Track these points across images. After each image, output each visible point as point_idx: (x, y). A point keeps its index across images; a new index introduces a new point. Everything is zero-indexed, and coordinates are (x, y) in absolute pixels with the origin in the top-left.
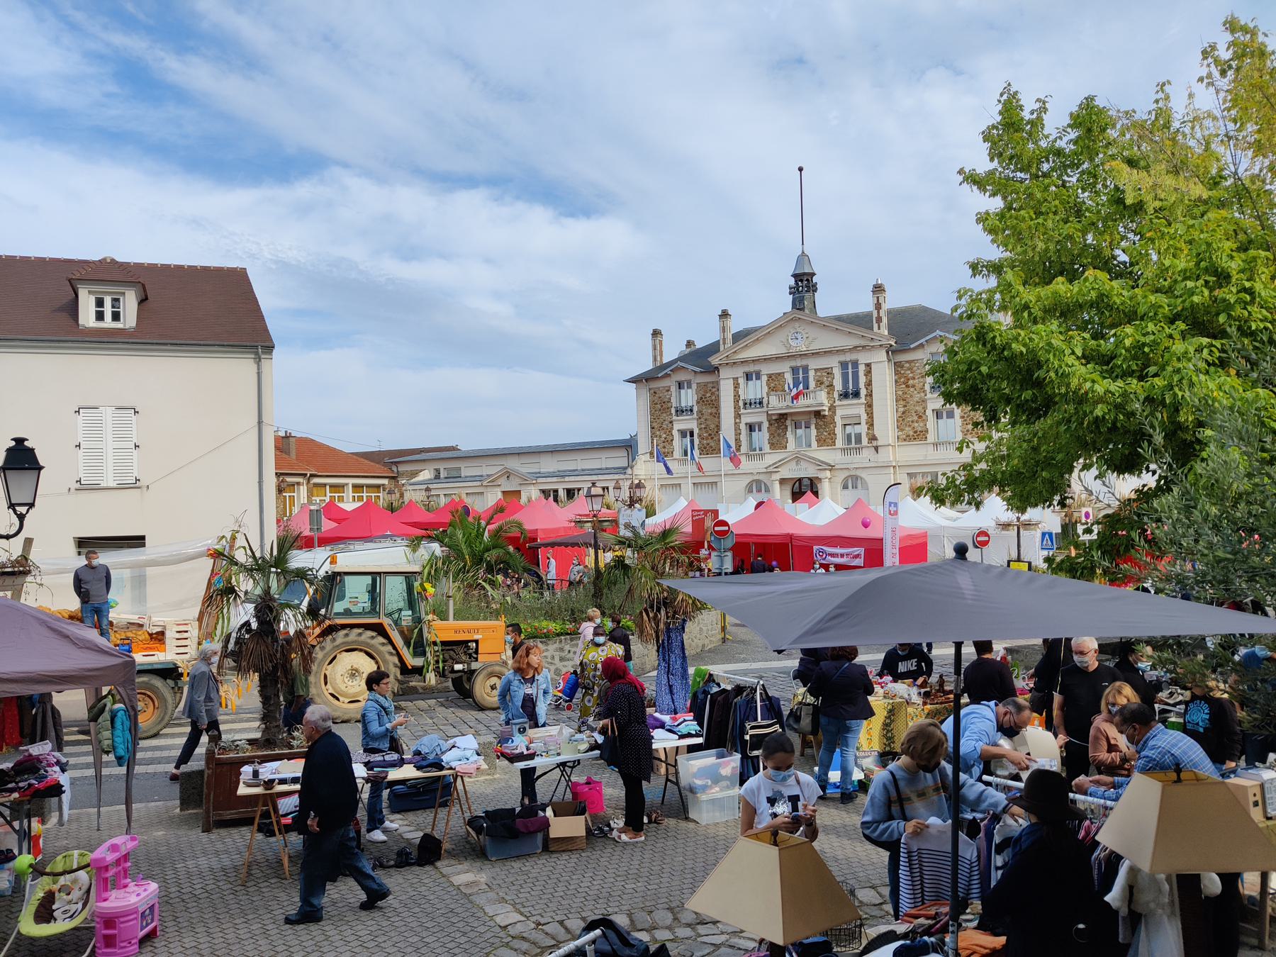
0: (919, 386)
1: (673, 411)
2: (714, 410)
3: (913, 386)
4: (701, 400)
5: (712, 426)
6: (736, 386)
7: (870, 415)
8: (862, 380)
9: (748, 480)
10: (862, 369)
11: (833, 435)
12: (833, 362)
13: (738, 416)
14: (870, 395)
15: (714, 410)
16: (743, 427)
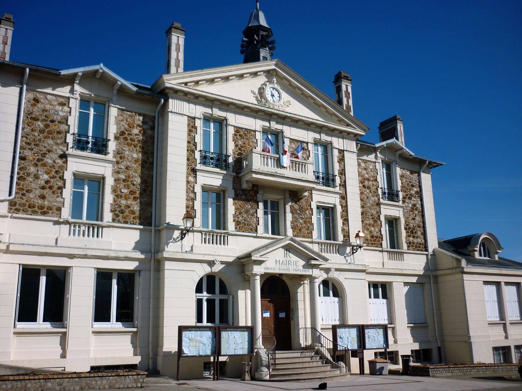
0: (373, 189)
1: (70, 139)
3: (369, 188)
6: (192, 129)
7: (345, 208)
8: (337, 167)
9: (204, 270)
10: (336, 153)
11: (308, 221)
12: (308, 136)
14: (344, 185)
16: (198, 189)
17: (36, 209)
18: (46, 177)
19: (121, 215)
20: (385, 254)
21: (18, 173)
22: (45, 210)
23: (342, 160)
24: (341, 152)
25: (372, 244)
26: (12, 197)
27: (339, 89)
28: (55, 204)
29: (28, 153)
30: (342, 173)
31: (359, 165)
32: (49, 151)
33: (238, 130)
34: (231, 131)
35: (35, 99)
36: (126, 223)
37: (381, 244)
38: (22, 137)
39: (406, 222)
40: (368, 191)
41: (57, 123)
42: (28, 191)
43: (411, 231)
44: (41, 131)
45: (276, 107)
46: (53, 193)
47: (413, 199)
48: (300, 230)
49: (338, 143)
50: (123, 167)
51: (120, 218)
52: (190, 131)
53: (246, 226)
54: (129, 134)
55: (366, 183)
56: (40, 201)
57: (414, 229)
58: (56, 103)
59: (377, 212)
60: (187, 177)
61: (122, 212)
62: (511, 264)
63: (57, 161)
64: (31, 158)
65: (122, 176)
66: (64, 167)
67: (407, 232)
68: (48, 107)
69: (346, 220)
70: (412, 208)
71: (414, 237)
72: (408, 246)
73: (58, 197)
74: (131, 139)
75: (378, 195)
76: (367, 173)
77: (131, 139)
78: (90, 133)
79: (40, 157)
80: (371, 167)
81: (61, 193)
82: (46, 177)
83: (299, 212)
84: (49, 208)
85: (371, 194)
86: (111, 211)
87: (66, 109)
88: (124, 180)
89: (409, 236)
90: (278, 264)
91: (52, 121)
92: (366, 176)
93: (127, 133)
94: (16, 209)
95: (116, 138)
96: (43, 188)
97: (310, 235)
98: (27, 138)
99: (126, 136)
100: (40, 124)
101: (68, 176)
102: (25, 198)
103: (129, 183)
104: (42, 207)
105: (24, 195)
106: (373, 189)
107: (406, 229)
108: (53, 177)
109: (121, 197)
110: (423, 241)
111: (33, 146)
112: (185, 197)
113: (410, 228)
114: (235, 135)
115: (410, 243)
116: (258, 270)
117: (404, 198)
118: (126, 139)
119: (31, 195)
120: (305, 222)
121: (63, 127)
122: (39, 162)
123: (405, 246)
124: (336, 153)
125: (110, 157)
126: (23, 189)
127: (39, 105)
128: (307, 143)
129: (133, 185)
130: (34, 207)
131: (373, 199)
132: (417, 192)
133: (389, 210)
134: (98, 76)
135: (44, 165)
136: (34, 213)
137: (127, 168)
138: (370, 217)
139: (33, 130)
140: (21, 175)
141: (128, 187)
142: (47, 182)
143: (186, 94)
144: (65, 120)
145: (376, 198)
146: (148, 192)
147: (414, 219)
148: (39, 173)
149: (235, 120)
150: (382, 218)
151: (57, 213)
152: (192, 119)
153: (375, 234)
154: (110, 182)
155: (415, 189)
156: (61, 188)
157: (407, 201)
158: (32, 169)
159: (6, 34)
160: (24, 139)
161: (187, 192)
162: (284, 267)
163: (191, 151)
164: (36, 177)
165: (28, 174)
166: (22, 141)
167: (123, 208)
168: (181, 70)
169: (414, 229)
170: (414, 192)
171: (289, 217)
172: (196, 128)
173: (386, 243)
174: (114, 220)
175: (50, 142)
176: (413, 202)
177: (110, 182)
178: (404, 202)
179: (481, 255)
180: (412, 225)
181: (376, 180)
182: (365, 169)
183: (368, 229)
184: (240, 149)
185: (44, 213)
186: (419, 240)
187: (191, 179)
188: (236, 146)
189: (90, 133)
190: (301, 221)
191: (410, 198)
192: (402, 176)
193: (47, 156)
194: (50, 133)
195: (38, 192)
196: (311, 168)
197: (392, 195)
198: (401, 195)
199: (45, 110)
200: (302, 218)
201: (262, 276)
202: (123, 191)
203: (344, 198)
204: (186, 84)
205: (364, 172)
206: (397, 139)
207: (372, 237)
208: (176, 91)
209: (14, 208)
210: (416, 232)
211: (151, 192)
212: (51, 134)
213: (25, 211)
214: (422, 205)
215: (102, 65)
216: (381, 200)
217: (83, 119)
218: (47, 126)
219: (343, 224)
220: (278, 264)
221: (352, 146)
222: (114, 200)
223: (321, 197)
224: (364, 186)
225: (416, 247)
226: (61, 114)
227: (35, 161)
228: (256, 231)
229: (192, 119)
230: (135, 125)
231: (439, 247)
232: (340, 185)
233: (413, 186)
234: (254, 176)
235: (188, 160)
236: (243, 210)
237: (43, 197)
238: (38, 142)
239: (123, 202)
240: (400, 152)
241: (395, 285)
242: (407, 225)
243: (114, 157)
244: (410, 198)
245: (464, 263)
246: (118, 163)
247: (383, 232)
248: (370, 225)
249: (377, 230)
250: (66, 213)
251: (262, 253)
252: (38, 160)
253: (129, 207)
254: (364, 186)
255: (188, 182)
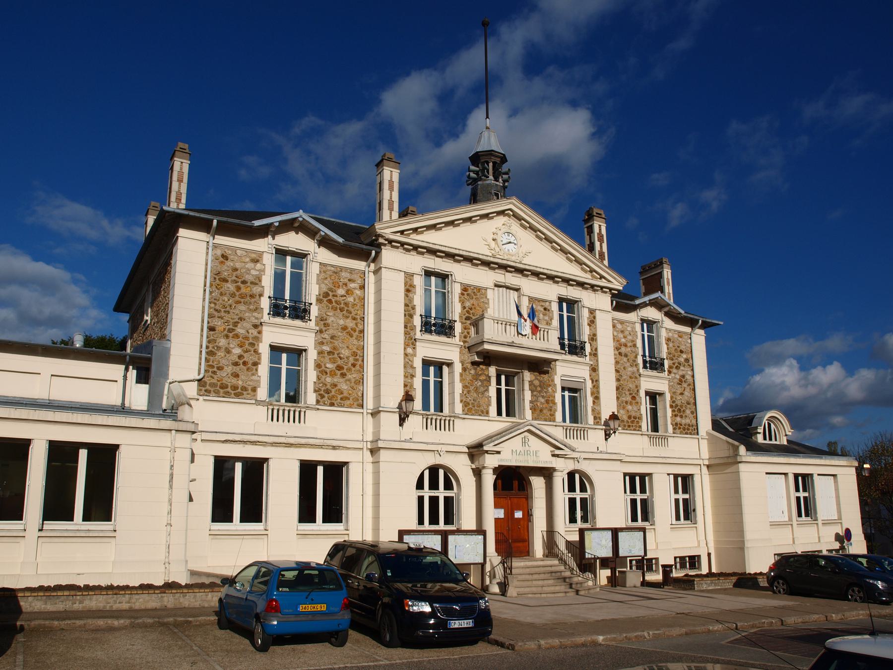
0: (632, 357)
1: (265, 304)
2: (350, 324)
3: (626, 356)
4: (325, 297)
5: (345, 353)
6: (409, 289)
7: (596, 382)
10: (585, 313)
11: (550, 401)
12: (550, 292)
13: (411, 342)
14: (594, 354)
15: (350, 324)
17: (229, 389)
18: (237, 351)
19: (326, 395)
20: (646, 438)
21: (207, 347)
22: (239, 390)
23: (592, 322)
24: (592, 312)
25: (629, 426)
26: (201, 376)
27: (590, 230)
28: (251, 383)
29: (218, 323)
30: (593, 338)
31: (614, 326)
32: (241, 319)
33: (465, 288)
34: (457, 289)
35: (223, 256)
36: (332, 405)
37: (640, 427)
38: (210, 303)
39: (672, 398)
40: (625, 359)
41: (249, 284)
42: (220, 368)
43: (678, 410)
44: (233, 295)
45: (513, 258)
46: (248, 369)
47: (682, 368)
48: (541, 411)
49: (588, 299)
50: (326, 336)
51: (326, 399)
52: (408, 291)
53: (474, 408)
54: (333, 296)
55: (623, 350)
56: (234, 381)
57: (681, 406)
58: (248, 260)
59: (637, 387)
60: (405, 349)
61: (328, 391)
62: (803, 450)
63: (250, 331)
64: (222, 328)
65: (326, 348)
66: (258, 339)
67: (673, 411)
68: (238, 265)
69: (596, 398)
70: (680, 380)
71: (681, 417)
72: (674, 429)
73: (253, 375)
74: (336, 302)
75: (637, 365)
76: (625, 337)
77: (336, 302)
78: (287, 297)
79: (231, 327)
80: (629, 329)
81: (257, 370)
82: (237, 351)
83: (539, 389)
84: (244, 389)
85: (628, 364)
86: (315, 391)
87: (259, 266)
88: (329, 353)
89: (676, 416)
90: (514, 454)
91: (244, 282)
92: (623, 340)
93: (331, 294)
94: (206, 391)
95: (319, 301)
96: (236, 364)
97: (552, 418)
98: (215, 304)
99: (330, 297)
100: (231, 287)
101: (264, 350)
102: (215, 376)
103: (336, 356)
104: (235, 388)
105: (214, 373)
106: (632, 357)
107: (671, 406)
108: (246, 352)
109: (326, 373)
110: (694, 422)
111: (223, 314)
112: (402, 374)
113: (677, 406)
114: (462, 294)
115: (676, 424)
116: (491, 462)
117: (670, 367)
118: (330, 301)
119: (223, 374)
120: (547, 402)
121: (256, 290)
122: (230, 333)
123: (670, 428)
124: (585, 313)
125: (312, 324)
126: (213, 367)
127: (229, 263)
128: (550, 302)
129: (341, 358)
130: (227, 387)
131: (630, 369)
132: (687, 360)
133: (652, 382)
134: (296, 225)
135: (237, 336)
136: (227, 394)
137: (333, 337)
138: (626, 391)
139: (221, 294)
140: (210, 349)
141: (333, 361)
142: (240, 357)
143: (403, 244)
144: (257, 281)
145: (635, 369)
146: (358, 367)
147: (682, 394)
148: (231, 346)
149: (463, 274)
150: (642, 394)
151: (252, 393)
152: (409, 276)
153: (633, 414)
154: (312, 355)
155: (685, 356)
156: (256, 364)
157: (674, 370)
158: (222, 342)
159: (181, 169)
160: (213, 305)
161: (405, 367)
162: (521, 458)
163: (409, 314)
164: (228, 351)
165: (219, 348)
166: (210, 308)
167: (329, 387)
168: (395, 215)
169: (681, 406)
170: (682, 360)
171: (528, 395)
172: (414, 287)
173: (645, 424)
174: (318, 402)
175: (242, 307)
176: (681, 373)
177: (312, 355)
178: (670, 372)
179: (765, 439)
180: (679, 403)
181: (635, 346)
182: (622, 332)
183: (624, 408)
184: (468, 312)
185: (238, 395)
186: (688, 421)
187: (409, 350)
188: (464, 308)
189: (287, 297)
190: (543, 400)
191: (677, 368)
192: (668, 340)
193: (239, 325)
194: (242, 296)
195: (229, 369)
196: (554, 335)
197: (655, 365)
198: (666, 363)
199: (236, 270)
200: (543, 397)
201: (495, 470)
202: (328, 365)
203: (594, 369)
204: (402, 232)
205: (621, 335)
206: (663, 292)
207: (630, 417)
208: (390, 242)
209: (203, 389)
210: (684, 411)
211: (362, 367)
212: (242, 298)
213: (217, 393)
214: (693, 376)
215: (301, 211)
216: (641, 370)
217: (279, 277)
218: (238, 288)
219: (594, 402)
220: (514, 454)
221: (603, 302)
222: (318, 378)
223: (568, 369)
224: (620, 354)
225: (684, 429)
226: (253, 272)
227: (226, 332)
228: (487, 413)
229: (409, 276)
230: (341, 284)
231: (713, 429)
232: (590, 354)
233: (681, 352)
234: (487, 347)
235: (406, 327)
236: (472, 388)
237: (236, 376)
238: (228, 309)
239: (329, 380)
240: (666, 309)
241: (655, 478)
242: (674, 402)
243: (317, 325)
244: (677, 368)
245: (742, 449)
246: (321, 331)
247: (643, 411)
248: (626, 402)
249: (635, 409)
250: (263, 393)
251: (496, 442)
252: (230, 331)
253: (336, 386)
254: (620, 354)
255: (406, 355)
